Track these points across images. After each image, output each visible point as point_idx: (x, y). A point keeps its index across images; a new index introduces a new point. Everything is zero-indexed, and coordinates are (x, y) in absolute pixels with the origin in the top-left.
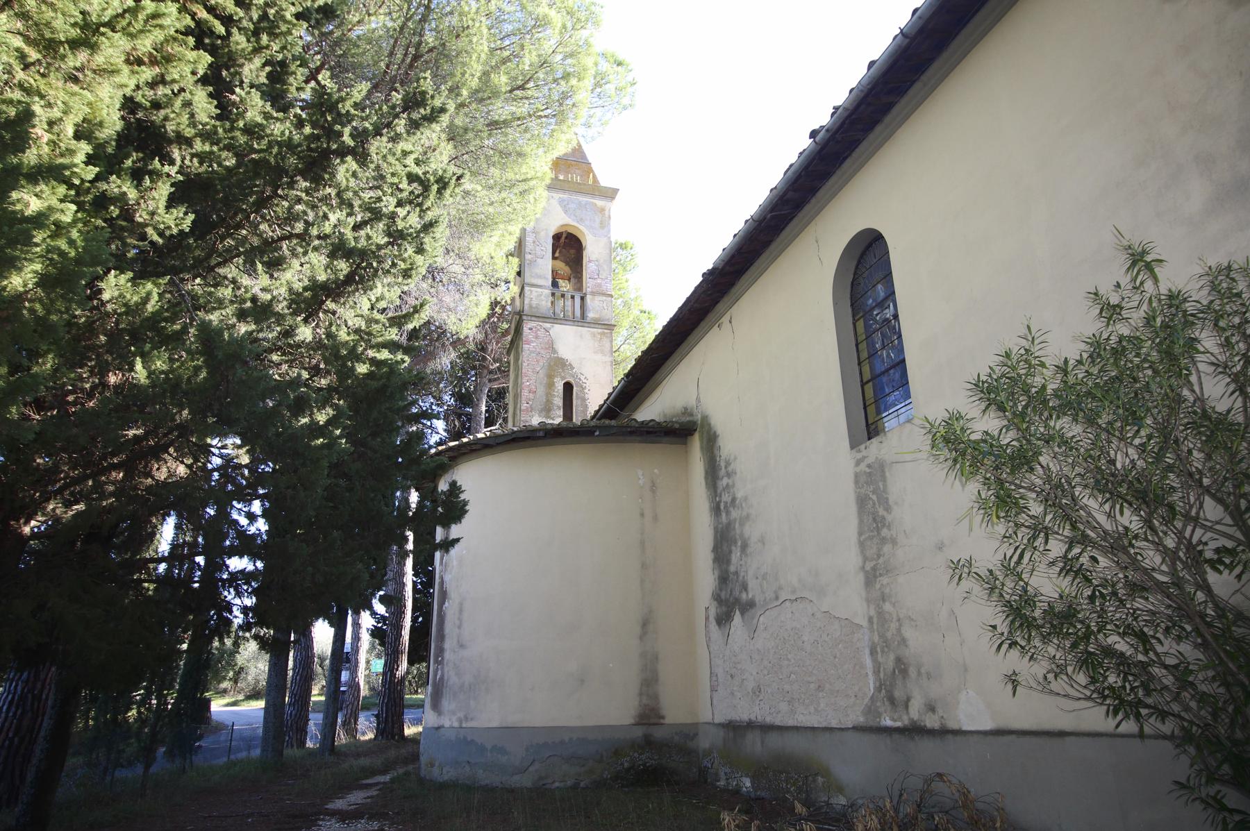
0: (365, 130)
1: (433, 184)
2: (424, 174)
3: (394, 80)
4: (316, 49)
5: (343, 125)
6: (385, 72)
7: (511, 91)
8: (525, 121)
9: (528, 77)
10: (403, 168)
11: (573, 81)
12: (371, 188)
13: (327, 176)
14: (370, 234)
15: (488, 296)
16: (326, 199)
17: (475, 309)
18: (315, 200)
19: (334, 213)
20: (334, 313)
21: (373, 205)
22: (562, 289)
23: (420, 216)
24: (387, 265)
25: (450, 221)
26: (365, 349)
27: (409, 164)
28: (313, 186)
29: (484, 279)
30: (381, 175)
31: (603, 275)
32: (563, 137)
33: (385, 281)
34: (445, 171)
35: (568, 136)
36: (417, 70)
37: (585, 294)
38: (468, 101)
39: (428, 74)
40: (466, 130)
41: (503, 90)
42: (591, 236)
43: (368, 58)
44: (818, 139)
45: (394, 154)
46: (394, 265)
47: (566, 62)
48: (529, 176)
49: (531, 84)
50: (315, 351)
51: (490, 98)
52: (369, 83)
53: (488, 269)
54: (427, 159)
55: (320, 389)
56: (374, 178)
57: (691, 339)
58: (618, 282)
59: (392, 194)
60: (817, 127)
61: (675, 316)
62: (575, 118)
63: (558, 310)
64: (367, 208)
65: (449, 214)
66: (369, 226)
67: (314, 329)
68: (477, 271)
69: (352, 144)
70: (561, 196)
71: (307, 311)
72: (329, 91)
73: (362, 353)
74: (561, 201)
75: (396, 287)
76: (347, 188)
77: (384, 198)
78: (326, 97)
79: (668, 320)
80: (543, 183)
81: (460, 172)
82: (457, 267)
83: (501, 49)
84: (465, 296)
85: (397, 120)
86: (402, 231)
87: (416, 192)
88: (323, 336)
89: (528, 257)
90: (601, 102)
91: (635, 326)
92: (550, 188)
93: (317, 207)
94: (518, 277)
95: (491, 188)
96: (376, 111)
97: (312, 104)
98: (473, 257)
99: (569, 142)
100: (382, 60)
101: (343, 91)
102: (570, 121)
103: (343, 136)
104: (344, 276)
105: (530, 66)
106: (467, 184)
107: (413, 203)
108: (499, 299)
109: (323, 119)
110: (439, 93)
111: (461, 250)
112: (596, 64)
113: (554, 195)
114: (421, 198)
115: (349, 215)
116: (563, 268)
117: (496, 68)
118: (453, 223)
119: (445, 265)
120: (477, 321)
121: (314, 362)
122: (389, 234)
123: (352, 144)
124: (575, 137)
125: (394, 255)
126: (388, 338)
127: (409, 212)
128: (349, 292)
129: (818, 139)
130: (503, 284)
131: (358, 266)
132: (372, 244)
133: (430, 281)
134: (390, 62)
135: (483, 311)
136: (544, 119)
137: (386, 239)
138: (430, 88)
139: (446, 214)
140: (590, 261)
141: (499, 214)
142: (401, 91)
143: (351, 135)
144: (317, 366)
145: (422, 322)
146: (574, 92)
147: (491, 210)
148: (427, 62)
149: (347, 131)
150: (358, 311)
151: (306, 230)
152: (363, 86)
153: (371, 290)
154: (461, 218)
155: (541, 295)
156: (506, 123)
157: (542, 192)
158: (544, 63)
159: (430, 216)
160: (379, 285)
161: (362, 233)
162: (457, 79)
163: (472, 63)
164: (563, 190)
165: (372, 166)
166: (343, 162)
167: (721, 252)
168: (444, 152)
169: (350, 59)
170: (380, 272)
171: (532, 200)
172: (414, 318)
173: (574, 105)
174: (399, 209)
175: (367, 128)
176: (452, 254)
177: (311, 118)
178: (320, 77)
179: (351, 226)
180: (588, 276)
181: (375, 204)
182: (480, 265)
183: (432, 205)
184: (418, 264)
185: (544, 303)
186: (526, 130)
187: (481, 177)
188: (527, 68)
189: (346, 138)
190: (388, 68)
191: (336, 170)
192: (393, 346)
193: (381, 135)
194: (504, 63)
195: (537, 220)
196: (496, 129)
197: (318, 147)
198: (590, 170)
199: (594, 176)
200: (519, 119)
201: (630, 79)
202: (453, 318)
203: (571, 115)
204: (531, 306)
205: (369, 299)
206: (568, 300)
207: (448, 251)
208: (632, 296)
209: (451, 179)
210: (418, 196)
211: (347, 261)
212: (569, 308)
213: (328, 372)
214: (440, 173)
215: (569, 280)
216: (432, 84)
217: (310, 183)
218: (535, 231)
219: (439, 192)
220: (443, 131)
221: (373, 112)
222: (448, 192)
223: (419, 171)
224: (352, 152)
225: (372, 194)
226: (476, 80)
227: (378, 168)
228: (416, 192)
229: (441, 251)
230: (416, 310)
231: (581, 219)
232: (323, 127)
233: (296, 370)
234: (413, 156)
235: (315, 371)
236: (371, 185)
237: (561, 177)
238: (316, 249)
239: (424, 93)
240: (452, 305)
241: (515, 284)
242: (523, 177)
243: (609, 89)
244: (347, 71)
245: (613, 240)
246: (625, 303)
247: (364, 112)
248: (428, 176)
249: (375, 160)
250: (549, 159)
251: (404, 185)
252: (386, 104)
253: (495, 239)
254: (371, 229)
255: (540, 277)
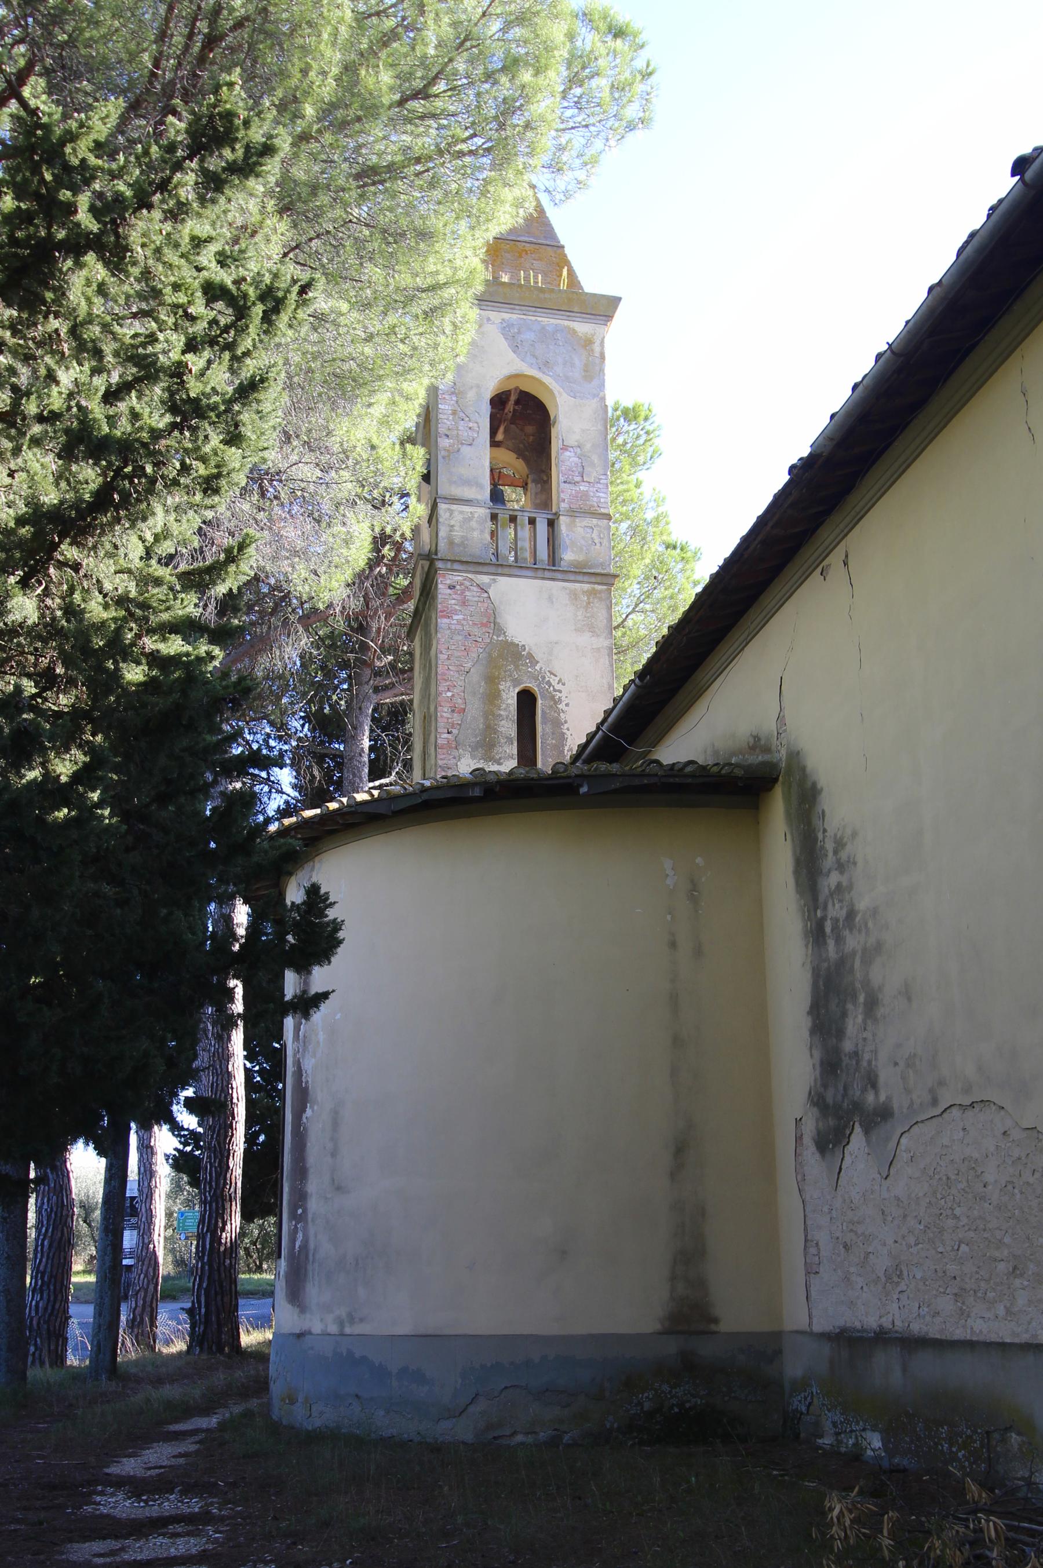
0: (118, 198)
1: (254, 304)
2: (237, 282)
3: (168, 91)
4: (16, 32)
5: (76, 190)
6: (153, 75)
7: (401, 103)
8: (431, 165)
9: (435, 70)
10: (195, 274)
11: (526, 76)
12: (135, 316)
13: (49, 296)
14: (138, 408)
15: (366, 525)
16: (50, 341)
17: (344, 551)
18: (30, 343)
19: (67, 368)
20: (76, 567)
21: (141, 350)
22: (509, 505)
23: (232, 370)
24: (172, 469)
25: (290, 377)
26: (139, 636)
27: (205, 263)
28: (25, 316)
29: (359, 490)
30: (153, 289)
31: (592, 474)
32: (508, 195)
33: (170, 501)
34: (276, 276)
35: (517, 192)
36: (215, 67)
37: (557, 515)
38: (315, 127)
39: (236, 76)
40: (314, 189)
41: (386, 101)
42: (565, 395)
43: (115, 48)
44: (1029, 174)
45: (177, 245)
46: (185, 469)
47: (510, 36)
48: (442, 279)
49: (441, 86)
50: (45, 641)
51: (359, 119)
52: (121, 99)
53: (366, 471)
54: (241, 251)
55: (58, 715)
56: (141, 296)
57: (768, 600)
58: (621, 487)
59: (176, 328)
60: (1027, 150)
61: (734, 553)
62: (531, 154)
63: (504, 549)
64: (130, 356)
65: (286, 362)
66: (133, 394)
67: (41, 599)
68: (345, 474)
69: (94, 227)
70: (506, 316)
71: (26, 564)
72: (45, 120)
73: (133, 644)
74: (506, 329)
75: (191, 513)
76: (89, 320)
77: (161, 336)
78: (39, 132)
79: (721, 563)
80: (470, 294)
81: (304, 276)
82: (306, 468)
83: (378, 14)
84: (324, 525)
85: (178, 175)
86: (197, 400)
87: (222, 322)
88: (59, 613)
89: (444, 443)
90: (583, 116)
91: (656, 575)
92: (483, 301)
93: (35, 358)
94: (424, 483)
95: (367, 306)
96: (137, 158)
97: (15, 148)
98: (336, 448)
99: (518, 204)
100: (145, 50)
101: (71, 117)
102: (521, 160)
103: (76, 212)
104: (91, 493)
105: (436, 47)
106: (321, 301)
107: (217, 343)
108: (388, 530)
109: (36, 179)
110: (258, 115)
111: (314, 434)
112: (571, 36)
113: (492, 315)
114: (232, 333)
115: (96, 371)
116: (513, 464)
117: (368, 56)
118: (296, 379)
119: (283, 465)
120: (348, 575)
121: (44, 662)
122: (173, 408)
123: (94, 227)
124: (530, 192)
125: (186, 450)
126: (180, 613)
127: (209, 362)
128: (102, 526)
129: (1029, 174)
130: (395, 499)
131: (118, 472)
132: (141, 428)
133: (255, 497)
134: (161, 53)
135: (359, 554)
136: (468, 159)
137: (168, 418)
138: (241, 104)
139: (281, 362)
140: (565, 448)
141: (386, 358)
142: (184, 114)
143: (92, 209)
144: (50, 668)
145: (244, 579)
146: (528, 99)
147: (368, 350)
148: (233, 50)
149: (84, 200)
150: (121, 561)
151: (16, 404)
152: (111, 107)
153: (144, 519)
154: (310, 370)
155: (470, 519)
156: (393, 170)
157: (468, 312)
158: (465, 40)
159: (250, 367)
160: (159, 510)
161: (122, 406)
162: (294, 82)
163: (322, 47)
164: (508, 304)
165: (135, 271)
166: (79, 265)
167: (872, 363)
168: (274, 238)
169: (83, 51)
170: (159, 485)
171: (448, 329)
172: (227, 573)
173: (527, 126)
174: (189, 357)
175: (122, 194)
176: (295, 443)
177: (13, 177)
178: (26, 92)
179: (100, 394)
180: (562, 479)
181: (145, 348)
182: (350, 463)
183: (254, 346)
184: (231, 467)
185: (476, 534)
186: (433, 185)
187: (347, 285)
188: (431, 51)
189: (84, 217)
190: (156, 65)
191: (67, 282)
192: (188, 628)
193: (150, 207)
194: (385, 45)
195: (459, 368)
196: (374, 184)
197: (29, 237)
198: (564, 261)
199: (571, 273)
200: (418, 160)
201: (640, 64)
202: (302, 570)
203: (522, 148)
204: (451, 543)
205: (140, 538)
206: (523, 527)
207: (287, 438)
208: (650, 515)
209: (288, 291)
210: (226, 329)
211: (95, 464)
212: (525, 544)
213: (71, 682)
214: (267, 279)
215: (525, 486)
216: (244, 96)
217: (20, 310)
218: (456, 391)
219: (267, 318)
220: (269, 193)
221: (132, 159)
222: (283, 320)
223: (225, 277)
224: (94, 243)
225: (138, 327)
226: (331, 81)
227: (146, 274)
228: (222, 322)
229: (273, 438)
230: (232, 557)
231: (547, 363)
232: (37, 196)
233: (13, 680)
234: (213, 248)
235: (47, 680)
236: (134, 309)
237: (505, 278)
238: (36, 442)
239: (229, 116)
240: (300, 544)
241: (419, 500)
242: (429, 281)
243: (601, 85)
244: (79, 77)
245: (610, 402)
246: (635, 531)
247: (115, 160)
248: (243, 287)
249: (140, 258)
250: (480, 242)
251: (199, 308)
252: (157, 143)
253: (378, 411)
254: (139, 398)
255: (467, 482)
